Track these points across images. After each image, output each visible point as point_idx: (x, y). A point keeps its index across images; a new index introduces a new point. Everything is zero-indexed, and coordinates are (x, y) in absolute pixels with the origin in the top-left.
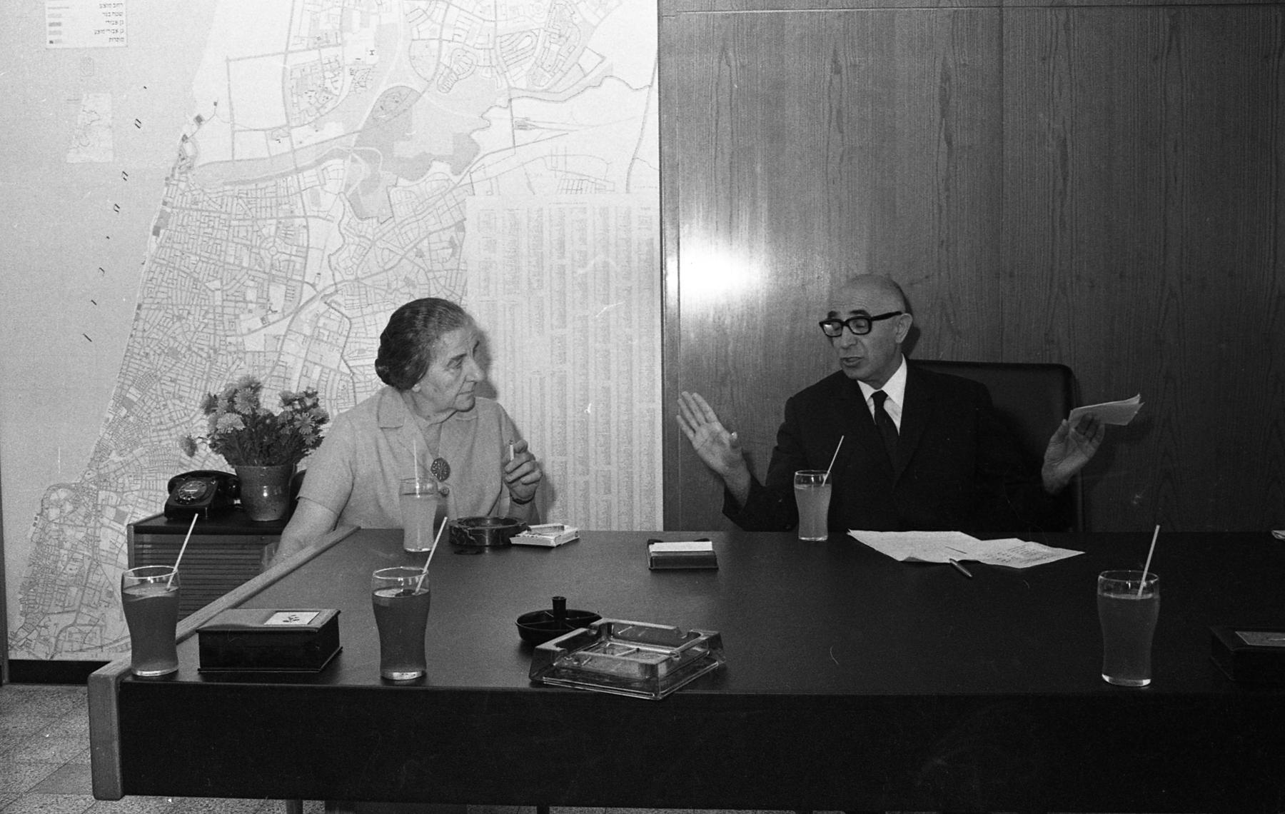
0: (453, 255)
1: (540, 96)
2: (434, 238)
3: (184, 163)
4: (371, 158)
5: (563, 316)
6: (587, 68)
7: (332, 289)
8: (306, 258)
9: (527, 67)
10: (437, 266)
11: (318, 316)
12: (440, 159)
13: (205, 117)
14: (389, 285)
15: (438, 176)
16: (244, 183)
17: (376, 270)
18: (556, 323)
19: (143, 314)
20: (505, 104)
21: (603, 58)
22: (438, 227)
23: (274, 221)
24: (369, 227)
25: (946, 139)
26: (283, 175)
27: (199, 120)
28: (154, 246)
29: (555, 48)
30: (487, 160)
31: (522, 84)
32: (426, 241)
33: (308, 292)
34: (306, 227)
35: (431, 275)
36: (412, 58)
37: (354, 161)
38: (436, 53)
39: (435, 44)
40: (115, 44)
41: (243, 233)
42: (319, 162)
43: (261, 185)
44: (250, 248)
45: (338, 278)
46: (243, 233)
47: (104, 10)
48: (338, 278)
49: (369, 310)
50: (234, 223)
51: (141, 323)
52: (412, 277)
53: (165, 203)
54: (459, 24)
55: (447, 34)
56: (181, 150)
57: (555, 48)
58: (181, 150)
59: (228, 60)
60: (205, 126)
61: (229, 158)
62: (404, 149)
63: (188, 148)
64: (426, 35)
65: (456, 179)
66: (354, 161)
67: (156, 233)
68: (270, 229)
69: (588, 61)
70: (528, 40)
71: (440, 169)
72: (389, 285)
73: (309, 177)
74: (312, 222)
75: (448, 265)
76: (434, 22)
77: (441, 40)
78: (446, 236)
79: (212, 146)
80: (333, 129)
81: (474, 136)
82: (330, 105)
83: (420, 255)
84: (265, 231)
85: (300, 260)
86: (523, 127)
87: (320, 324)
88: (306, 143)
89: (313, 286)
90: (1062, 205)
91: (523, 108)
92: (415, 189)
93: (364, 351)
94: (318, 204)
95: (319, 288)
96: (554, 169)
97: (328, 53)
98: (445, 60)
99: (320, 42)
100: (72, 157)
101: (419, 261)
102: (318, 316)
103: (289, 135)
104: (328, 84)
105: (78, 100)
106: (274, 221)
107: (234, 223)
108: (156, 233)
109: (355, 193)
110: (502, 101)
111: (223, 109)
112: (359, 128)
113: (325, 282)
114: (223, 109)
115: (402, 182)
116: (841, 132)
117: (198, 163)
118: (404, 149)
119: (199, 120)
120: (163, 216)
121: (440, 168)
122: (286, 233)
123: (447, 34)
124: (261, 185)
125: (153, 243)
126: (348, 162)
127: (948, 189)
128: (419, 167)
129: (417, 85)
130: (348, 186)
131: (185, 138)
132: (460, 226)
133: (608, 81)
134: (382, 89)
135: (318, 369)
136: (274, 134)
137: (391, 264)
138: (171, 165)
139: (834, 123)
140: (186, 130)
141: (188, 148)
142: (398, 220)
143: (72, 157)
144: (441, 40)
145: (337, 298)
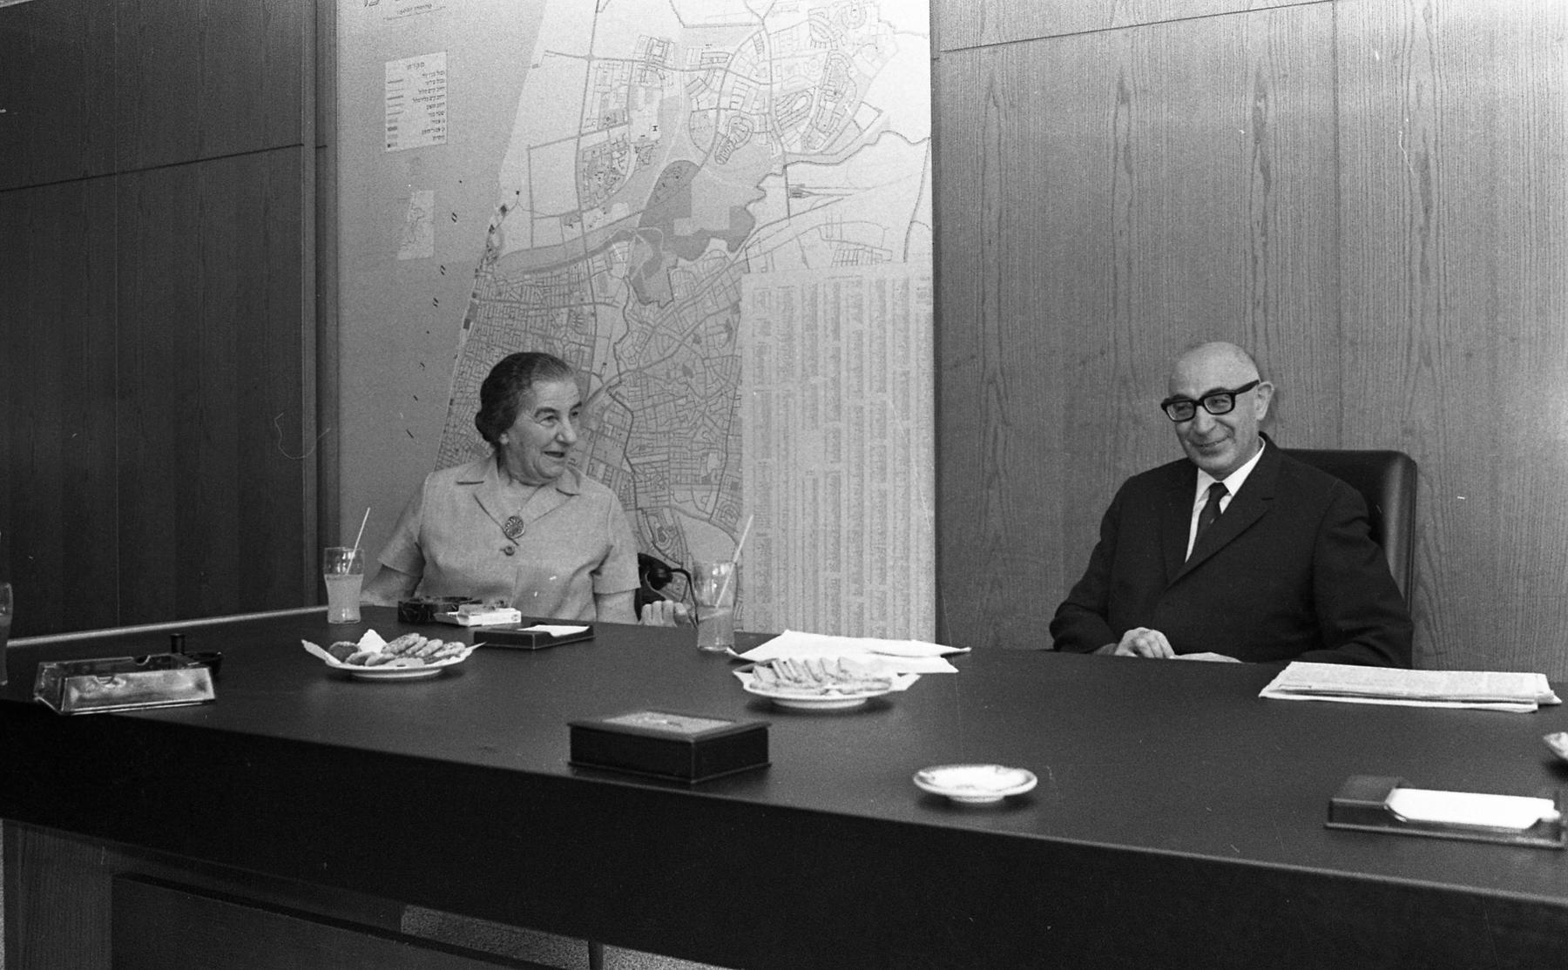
0: (729, 338)
1: (813, 159)
2: (710, 322)
3: (491, 254)
4: (654, 241)
5: (838, 408)
6: (863, 123)
7: (616, 381)
8: (593, 348)
9: (802, 129)
10: (714, 354)
11: (604, 409)
12: (716, 235)
13: (509, 207)
14: (668, 374)
15: (717, 254)
16: (541, 270)
17: (655, 359)
18: (832, 415)
19: (454, 408)
20: (779, 172)
21: (880, 111)
22: (715, 309)
23: (565, 310)
24: (650, 313)
25: (1262, 169)
26: (575, 261)
27: (504, 209)
28: (464, 340)
29: (830, 106)
30: (765, 232)
31: (797, 148)
32: (702, 327)
33: (595, 383)
34: (594, 315)
35: (707, 362)
36: (691, 130)
37: (638, 241)
38: (713, 123)
39: (712, 114)
40: (437, 141)
41: (539, 324)
42: (607, 244)
43: (556, 272)
44: (543, 337)
45: (622, 369)
46: (539, 324)
47: (435, 110)
48: (622, 369)
49: (648, 403)
50: (532, 313)
51: (452, 418)
52: (689, 365)
53: (474, 296)
54: (736, 91)
55: (725, 102)
56: (488, 240)
57: (830, 106)
58: (488, 240)
59: (529, 148)
60: (510, 215)
61: (528, 246)
62: (683, 228)
63: (495, 238)
64: (703, 106)
65: (732, 256)
66: (638, 241)
67: (466, 326)
68: (563, 319)
69: (865, 117)
70: (802, 102)
71: (718, 245)
72: (668, 374)
73: (598, 262)
74: (600, 308)
75: (727, 351)
76: (712, 91)
77: (718, 109)
78: (722, 321)
79: (516, 235)
80: (619, 211)
81: (750, 208)
82: (617, 186)
83: (697, 341)
84: (558, 320)
85: (588, 350)
86: (797, 194)
87: (606, 418)
88: (596, 226)
89: (600, 376)
90: (1424, 245)
91: (798, 174)
92: (694, 269)
93: (642, 448)
94: (604, 290)
95: (605, 379)
96: (829, 239)
97: (616, 132)
98: (722, 130)
99: (609, 122)
100: (404, 255)
101: (696, 347)
102: (604, 409)
103: (581, 220)
104: (615, 164)
105: (406, 200)
106: (565, 310)
107: (532, 313)
108: (466, 326)
109: (639, 279)
110: (777, 169)
111: (524, 196)
112: (643, 207)
113: (610, 373)
114: (524, 196)
115: (682, 262)
116: (1130, 172)
117: (504, 253)
118: (683, 228)
119: (504, 209)
120: (473, 308)
121: (718, 245)
122: (576, 321)
123: (725, 102)
124: (556, 272)
125: (464, 336)
126: (632, 246)
127: (1264, 234)
128: (694, 247)
129: (696, 161)
130: (632, 270)
131: (492, 229)
132: (736, 308)
133: (884, 136)
134: (663, 166)
135: (603, 466)
136: (570, 219)
137: (671, 351)
138: (480, 255)
139: (1121, 161)
140: (493, 221)
141: (496, 243)
142: (677, 303)
143: (404, 255)
144: (718, 109)
145: (621, 389)
